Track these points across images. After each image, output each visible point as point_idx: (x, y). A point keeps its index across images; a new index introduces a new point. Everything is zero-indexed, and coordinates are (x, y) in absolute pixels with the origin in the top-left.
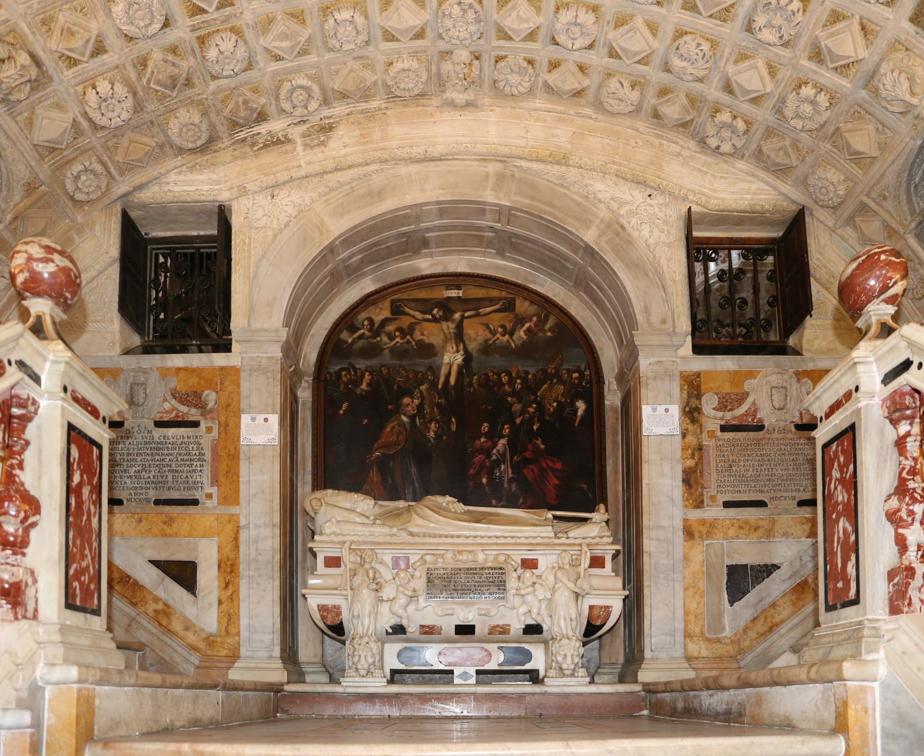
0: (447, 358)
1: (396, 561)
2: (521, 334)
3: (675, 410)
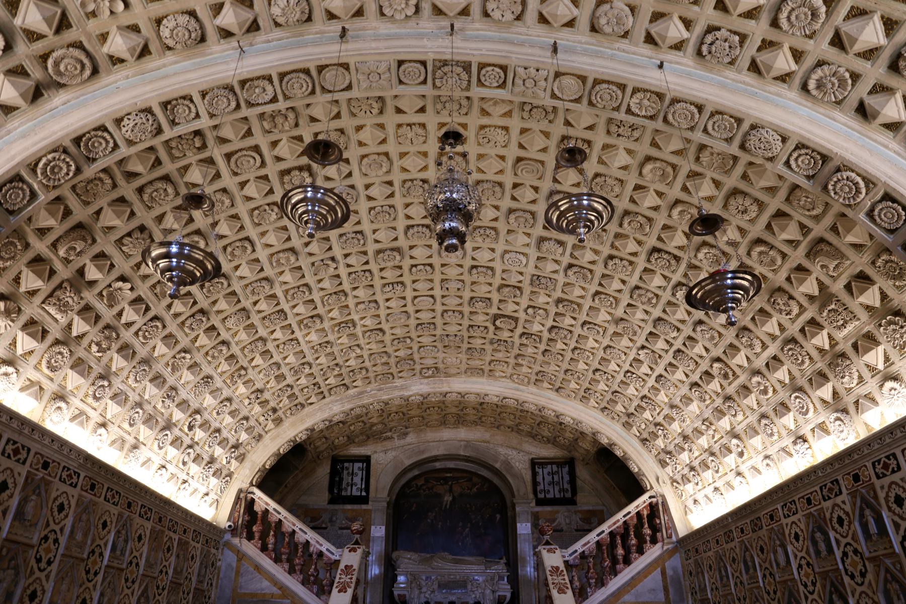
0: (446, 499)
1: (427, 578)
3: (529, 525)
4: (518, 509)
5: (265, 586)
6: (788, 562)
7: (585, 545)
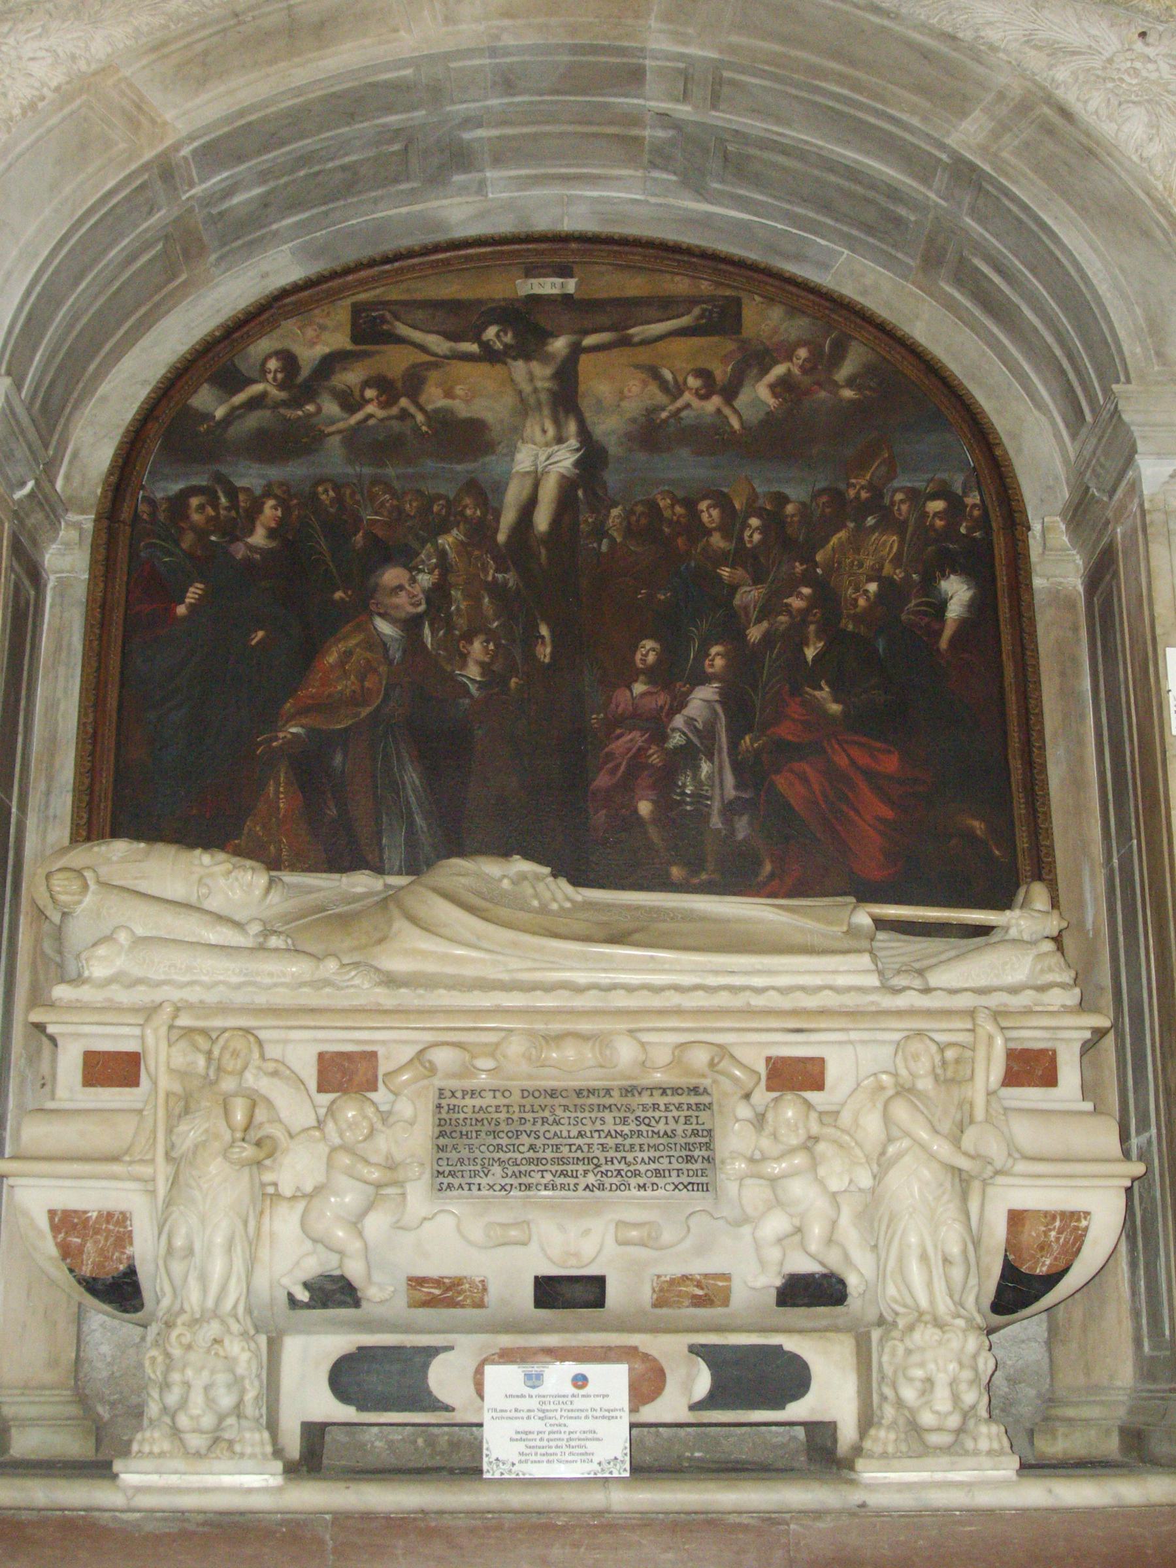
0: (524, 459)
2: (759, 394)
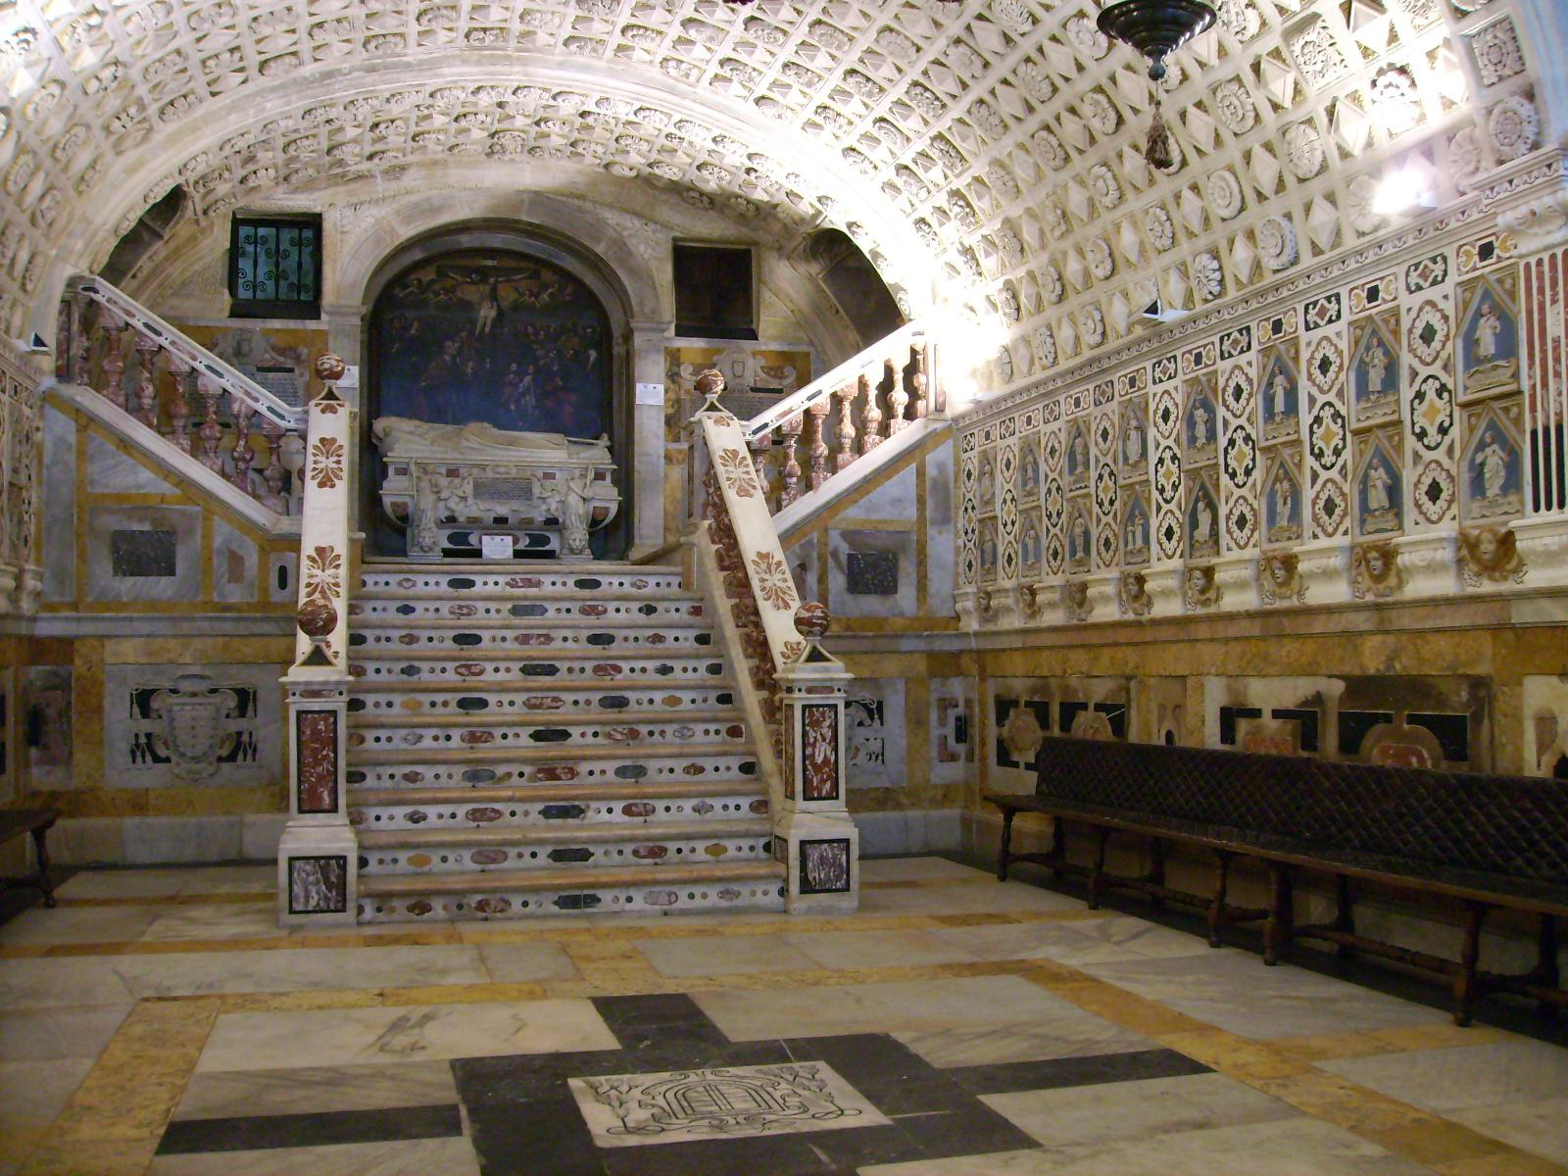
0: (483, 313)
2: (545, 297)
4: (638, 340)
5: (144, 478)
6: (1144, 454)
7: (785, 414)
